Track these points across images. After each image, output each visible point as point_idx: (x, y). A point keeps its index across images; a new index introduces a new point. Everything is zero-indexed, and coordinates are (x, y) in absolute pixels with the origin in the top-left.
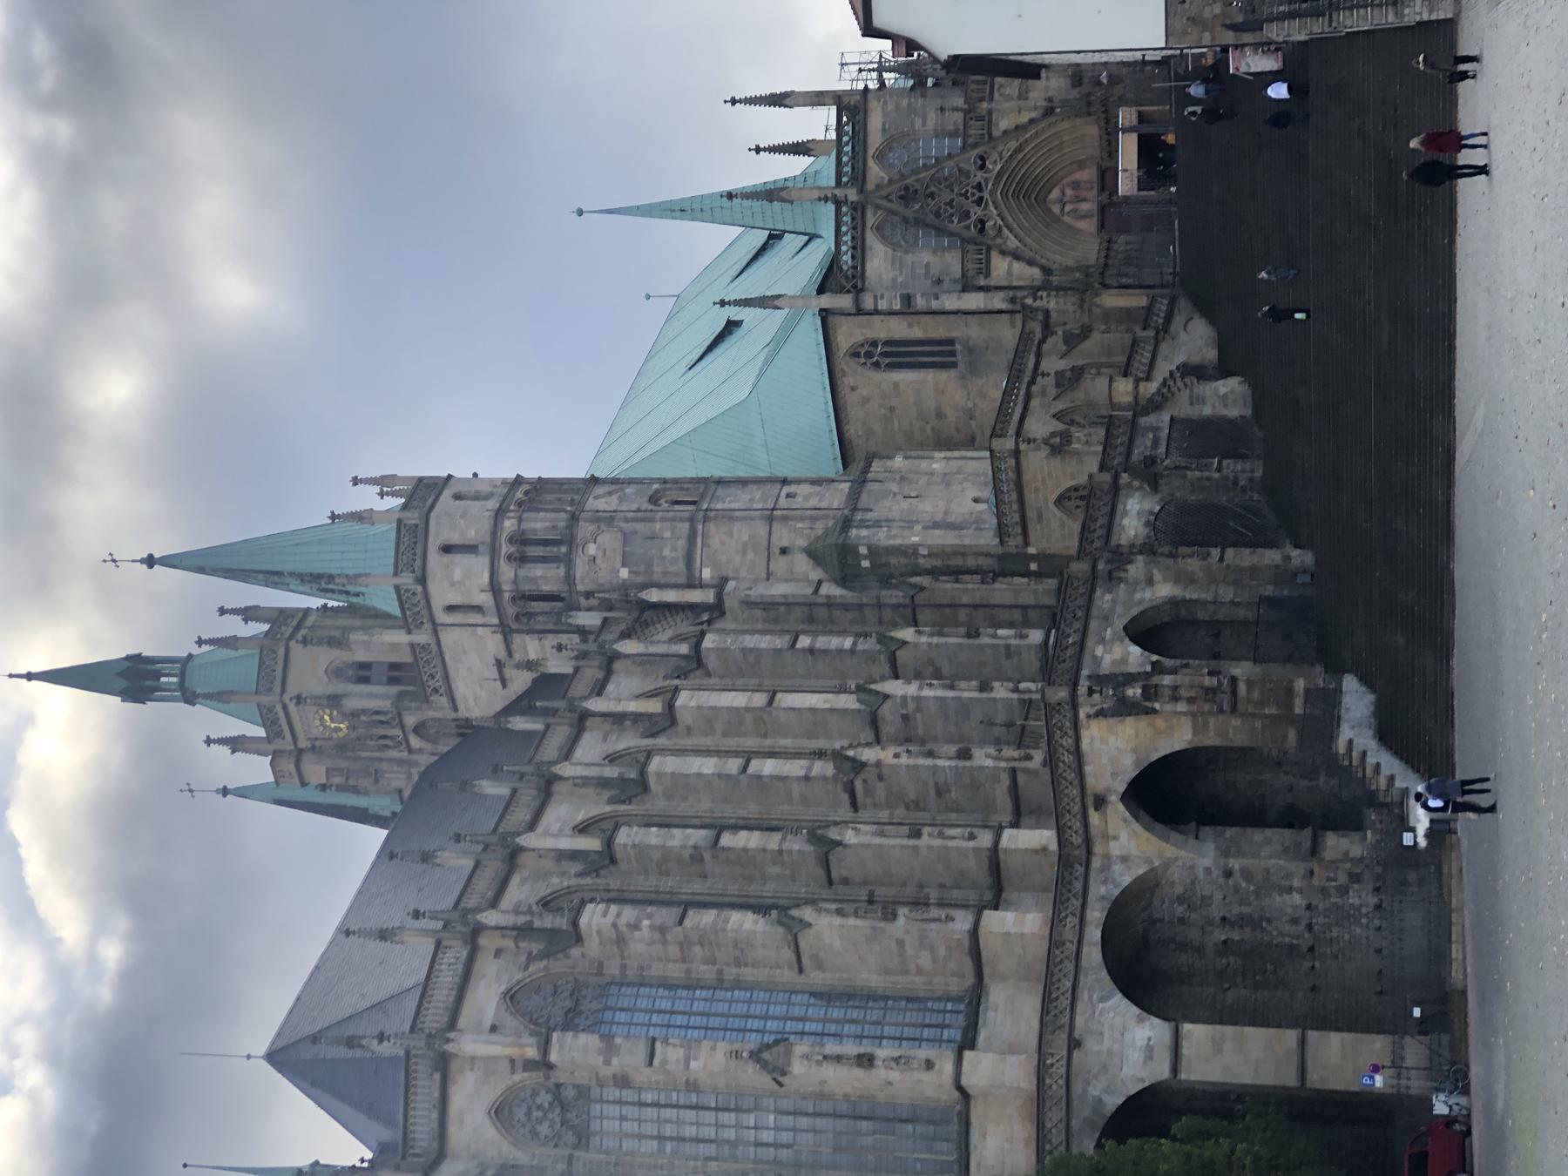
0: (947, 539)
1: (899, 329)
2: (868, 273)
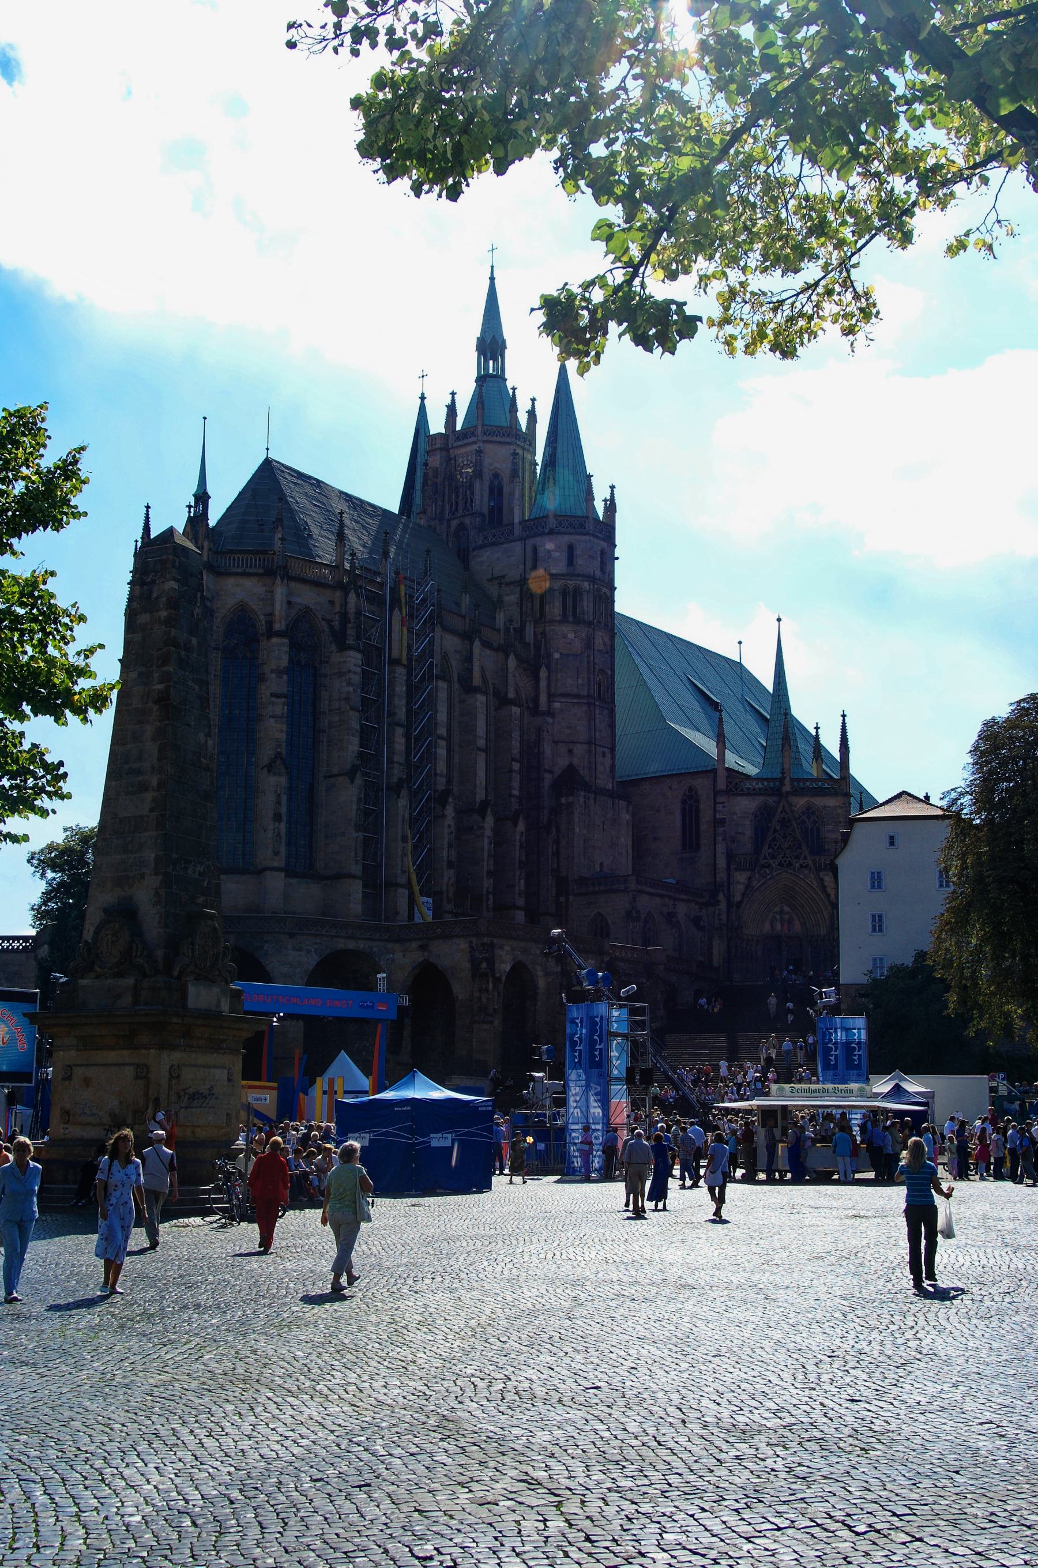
1: (706, 816)
2: (739, 798)
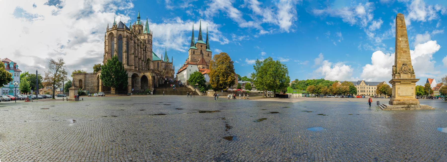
1: (160, 64)
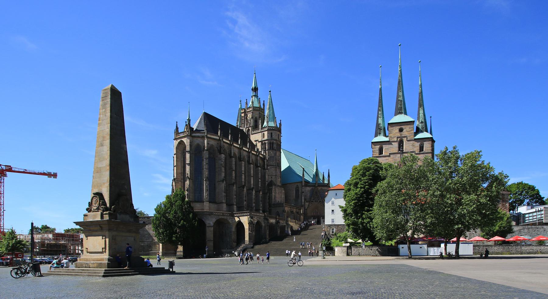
0: (273, 197)
1: (300, 191)
